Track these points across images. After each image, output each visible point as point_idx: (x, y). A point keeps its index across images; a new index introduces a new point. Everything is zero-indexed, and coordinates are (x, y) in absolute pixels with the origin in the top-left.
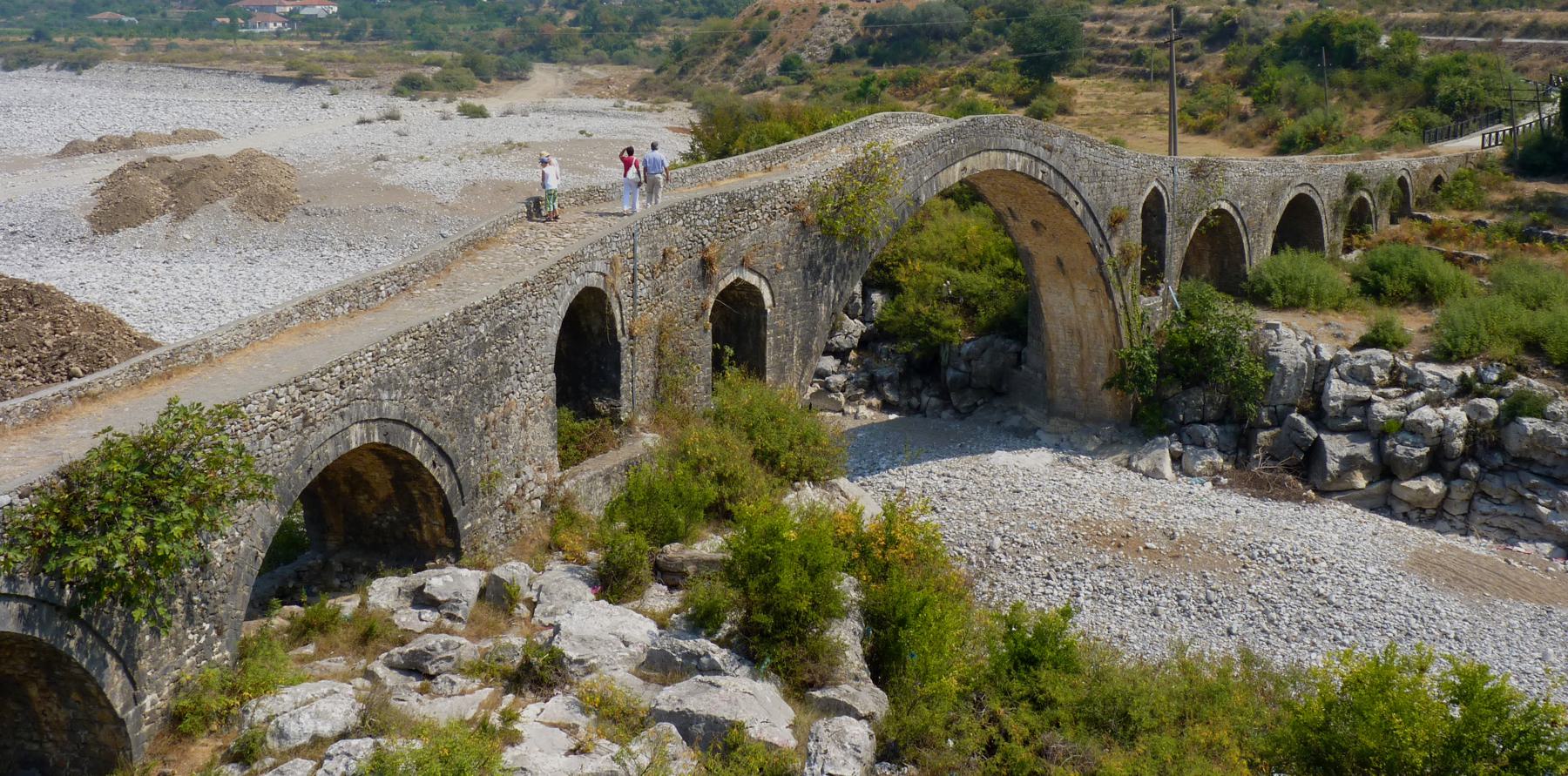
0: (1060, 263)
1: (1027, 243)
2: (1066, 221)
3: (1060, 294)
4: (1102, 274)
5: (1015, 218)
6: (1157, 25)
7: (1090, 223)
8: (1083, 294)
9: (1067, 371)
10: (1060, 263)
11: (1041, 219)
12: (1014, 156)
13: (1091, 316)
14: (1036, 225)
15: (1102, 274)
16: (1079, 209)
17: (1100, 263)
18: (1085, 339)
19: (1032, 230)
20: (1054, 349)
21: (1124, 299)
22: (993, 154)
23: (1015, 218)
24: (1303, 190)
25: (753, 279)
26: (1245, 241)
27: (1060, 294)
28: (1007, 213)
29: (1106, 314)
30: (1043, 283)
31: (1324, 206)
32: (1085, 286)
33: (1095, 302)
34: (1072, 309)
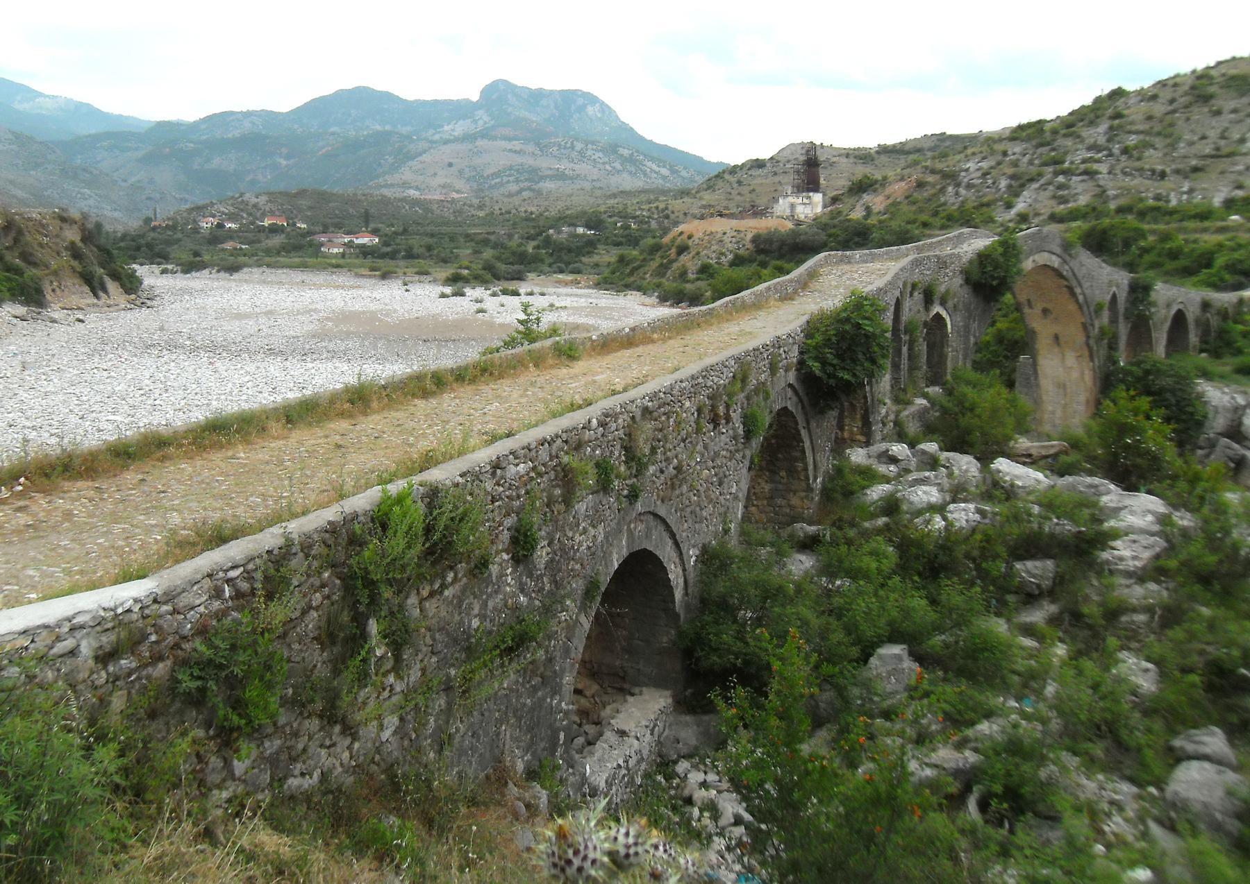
0: (1056, 338)
4: (1088, 345)
5: (1030, 306)
8: (1071, 359)
9: (1053, 413)
10: (1056, 338)
12: (1054, 257)
13: (1075, 375)
14: (1045, 311)
16: (1081, 298)
18: (1069, 390)
20: (1044, 397)
22: (1046, 255)
24: (1181, 307)
25: (944, 314)
28: (1026, 303)
29: (1087, 372)
30: (1041, 352)
31: (1191, 316)
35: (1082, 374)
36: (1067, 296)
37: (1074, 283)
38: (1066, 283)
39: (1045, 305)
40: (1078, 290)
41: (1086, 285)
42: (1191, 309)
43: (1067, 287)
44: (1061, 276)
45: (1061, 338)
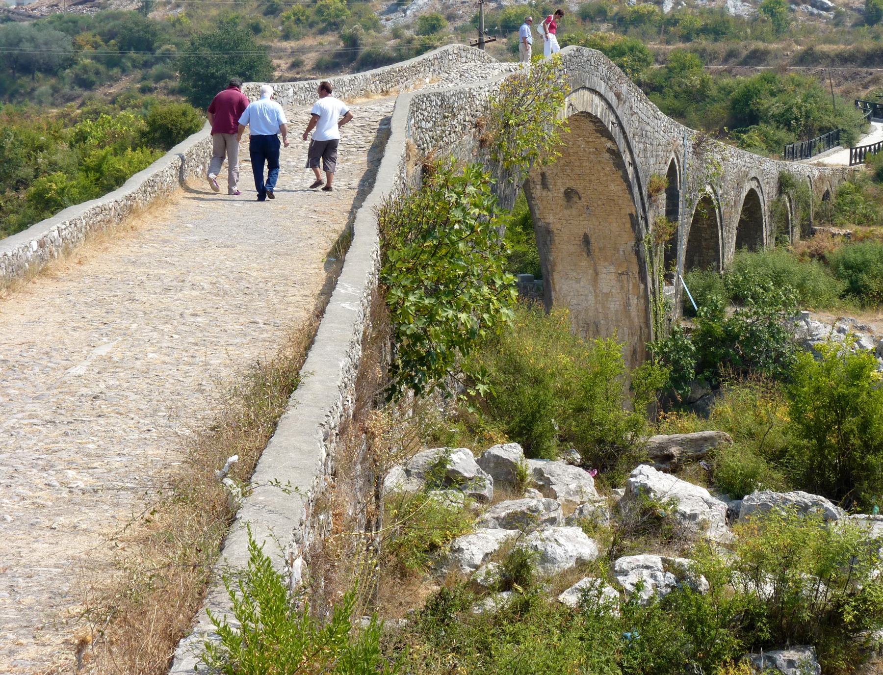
1: (550, 219)
2: (612, 187)
3: (578, 281)
4: (638, 253)
5: (545, 185)
6: (327, 58)
7: (636, 190)
8: (608, 279)
11: (578, 186)
13: (614, 306)
15: (638, 253)
16: (630, 170)
17: (639, 239)
19: (562, 202)
21: (653, 285)
23: (545, 185)
26: (720, 234)
27: (578, 281)
28: (538, 179)
29: (634, 301)
30: (559, 268)
32: (612, 269)
33: (622, 287)
34: (591, 298)
35: (627, 305)
36: (609, 167)
37: (622, 146)
38: (609, 145)
39: (571, 184)
40: (627, 158)
41: (637, 147)
42: (766, 189)
43: (609, 151)
44: (604, 132)
45: (592, 240)
